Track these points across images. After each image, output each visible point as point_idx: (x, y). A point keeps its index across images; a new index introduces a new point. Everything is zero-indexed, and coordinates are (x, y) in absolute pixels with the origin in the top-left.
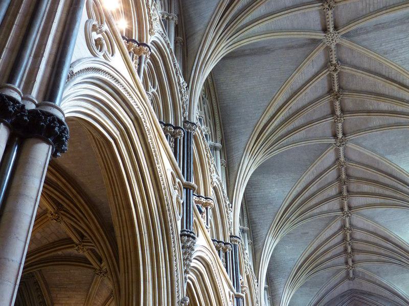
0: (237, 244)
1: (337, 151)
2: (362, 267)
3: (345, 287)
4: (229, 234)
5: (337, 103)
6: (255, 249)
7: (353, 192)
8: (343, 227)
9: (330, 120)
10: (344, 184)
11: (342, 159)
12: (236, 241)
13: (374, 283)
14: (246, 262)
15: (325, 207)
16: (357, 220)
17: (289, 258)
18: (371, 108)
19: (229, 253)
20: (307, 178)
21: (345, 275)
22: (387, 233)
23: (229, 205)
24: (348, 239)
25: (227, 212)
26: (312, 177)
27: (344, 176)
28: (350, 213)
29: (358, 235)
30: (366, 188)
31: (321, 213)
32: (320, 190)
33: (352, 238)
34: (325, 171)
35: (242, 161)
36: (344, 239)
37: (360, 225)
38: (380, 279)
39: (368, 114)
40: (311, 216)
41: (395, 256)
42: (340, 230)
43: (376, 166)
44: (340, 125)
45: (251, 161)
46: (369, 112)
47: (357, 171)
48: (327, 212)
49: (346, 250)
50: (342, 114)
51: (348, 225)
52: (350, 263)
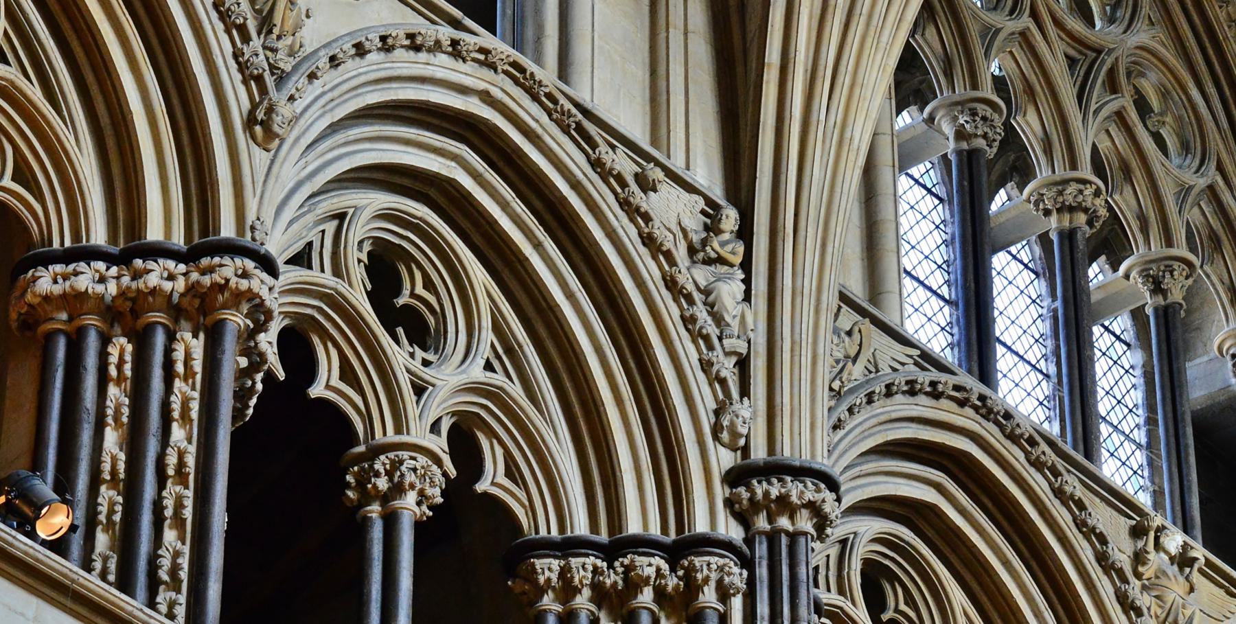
0: (805, 523)
4: (724, 459)
12: (784, 505)
25: (671, 284)
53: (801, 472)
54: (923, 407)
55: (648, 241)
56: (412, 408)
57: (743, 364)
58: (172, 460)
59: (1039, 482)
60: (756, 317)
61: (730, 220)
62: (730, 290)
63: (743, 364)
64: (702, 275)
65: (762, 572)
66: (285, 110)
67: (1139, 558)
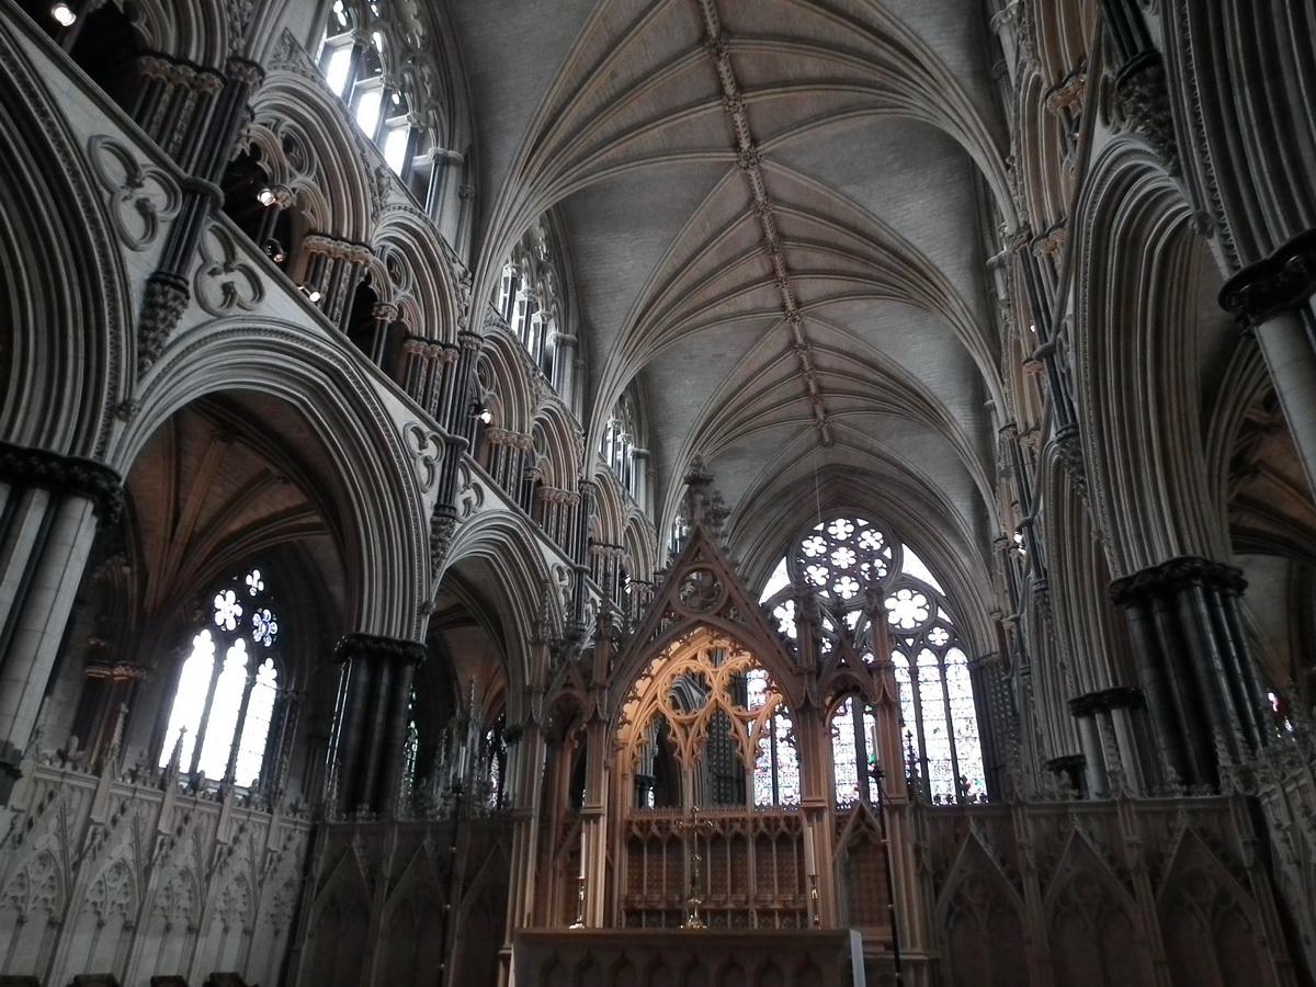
0: (475, 348)
1: (747, 178)
2: (840, 421)
3: (817, 459)
4: (459, 328)
5: (723, 67)
6: (589, 375)
7: (796, 270)
8: (792, 344)
9: (714, 107)
10: (774, 253)
11: (760, 198)
13: (869, 452)
14: (535, 393)
15: (746, 300)
16: (818, 332)
17: (691, 402)
18: (790, 73)
19: (452, 365)
20: (688, 238)
21: (815, 438)
22: (868, 353)
23: (466, 273)
24: (807, 368)
26: (702, 238)
27: (770, 236)
28: (798, 314)
29: (826, 359)
30: (819, 259)
31: (741, 313)
32: (726, 264)
33: (816, 367)
34: (729, 223)
35: (504, 188)
36: (800, 368)
37: (824, 339)
38: (876, 443)
39: (785, 89)
40: (719, 319)
41: (890, 396)
42: (786, 350)
43: (826, 210)
44: (738, 118)
45: (526, 189)
46: (787, 83)
47: (794, 223)
48: (753, 312)
49: (808, 389)
50: (738, 94)
51: (800, 340)
52: (821, 416)
53: (477, 336)
54: (498, 330)
55: (452, 274)
56: (393, 296)
57: (467, 308)
58: (340, 292)
59: (518, 354)
60: (471, 299)
61: (470, 275)
62: (467, 291)
63: (467, 308)
64: (461, 286)
65: (463, 356)
66: (382, 216)
67: (534, 375)
